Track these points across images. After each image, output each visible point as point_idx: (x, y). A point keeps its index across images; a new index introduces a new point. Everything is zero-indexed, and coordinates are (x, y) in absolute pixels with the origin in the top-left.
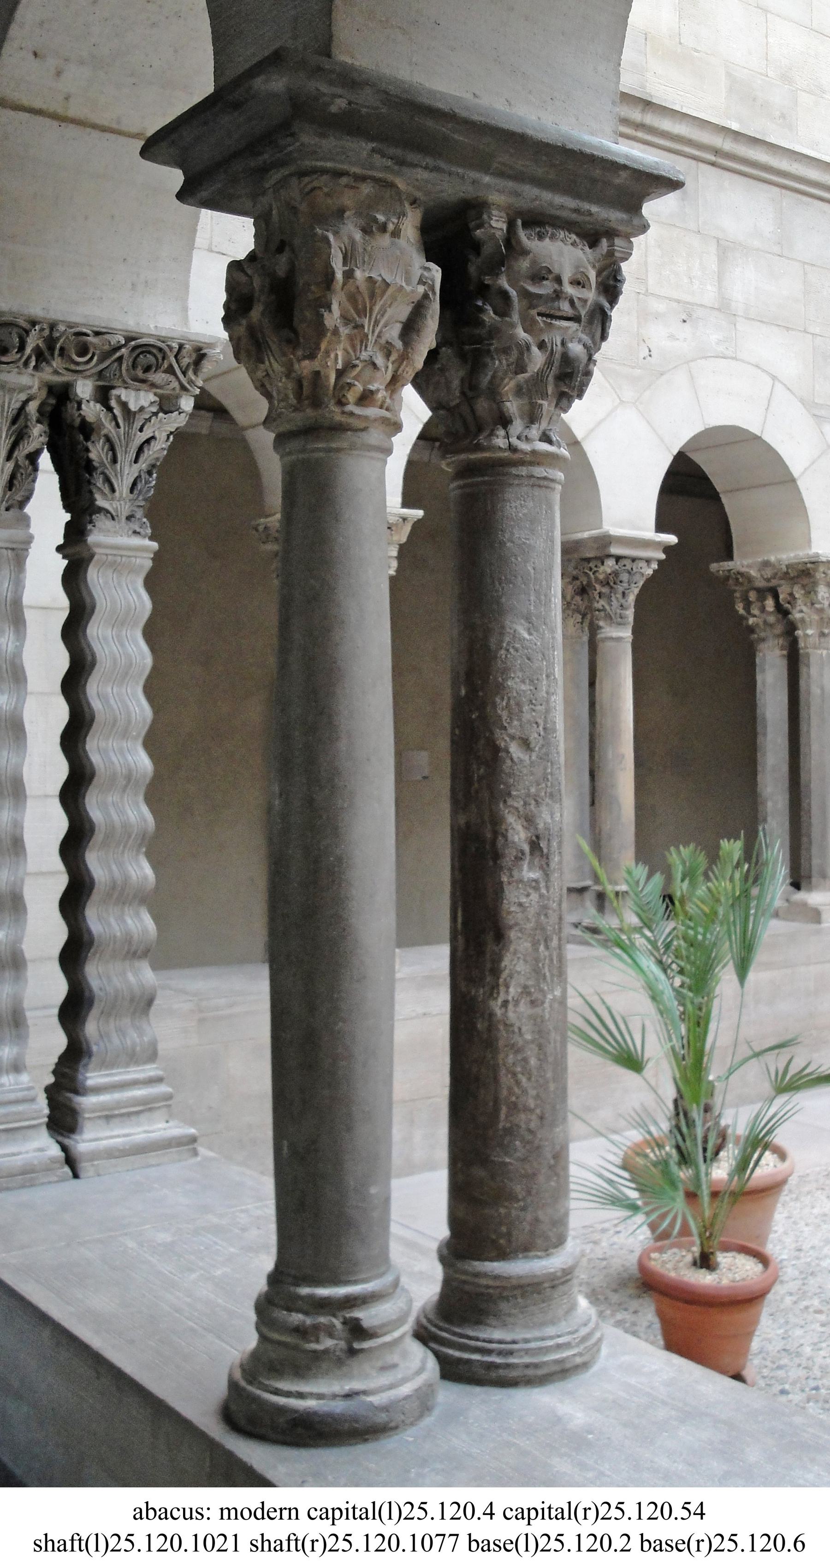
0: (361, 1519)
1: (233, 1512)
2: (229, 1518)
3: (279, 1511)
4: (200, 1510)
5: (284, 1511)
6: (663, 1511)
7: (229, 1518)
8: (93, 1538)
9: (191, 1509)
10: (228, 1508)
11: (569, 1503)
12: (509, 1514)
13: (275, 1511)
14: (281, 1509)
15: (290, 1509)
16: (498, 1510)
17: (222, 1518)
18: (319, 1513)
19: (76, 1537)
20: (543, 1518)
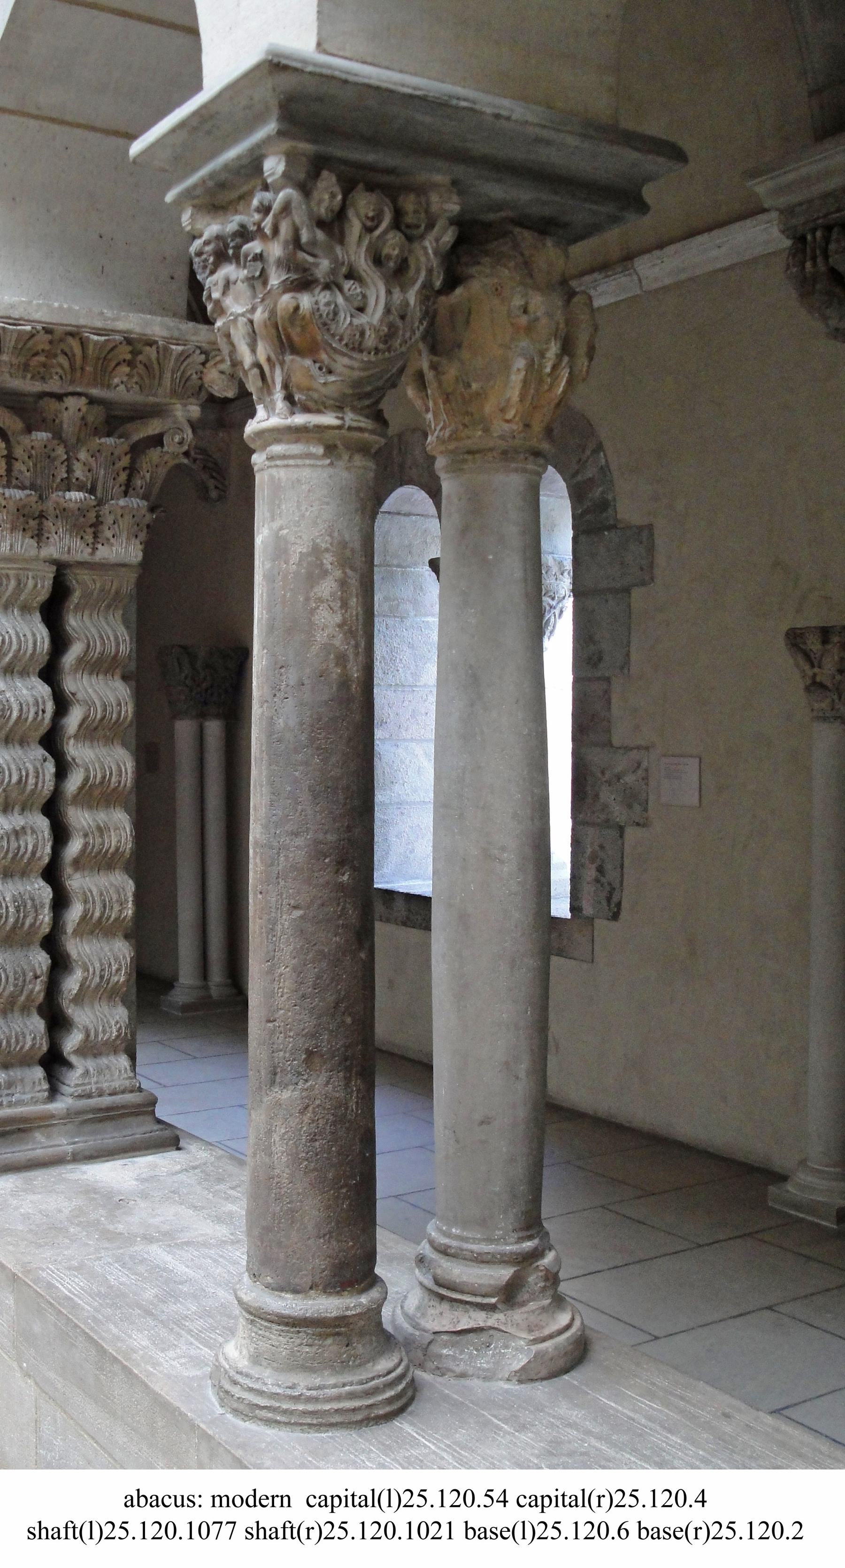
0: (360, 1506)
1: (224, 1500)
2: (221, 1506)
3: (271, 1498)
4: (191, 1498)
5: (276, 1499)
6: (677, 1498)
7: (221, 1506)
8: (87, 1526)
9: (183, 1497)
10: (219, 1496)
11: (583, 1490)
12: (522, 1501)
13: (267, 1498)
14: (273, 1497)
15: (282, 1497)
16: (511, 1498)
17: (214, 1506)
18: (528, 1500)
19: (288, 1525)
20: (557, 1506)
